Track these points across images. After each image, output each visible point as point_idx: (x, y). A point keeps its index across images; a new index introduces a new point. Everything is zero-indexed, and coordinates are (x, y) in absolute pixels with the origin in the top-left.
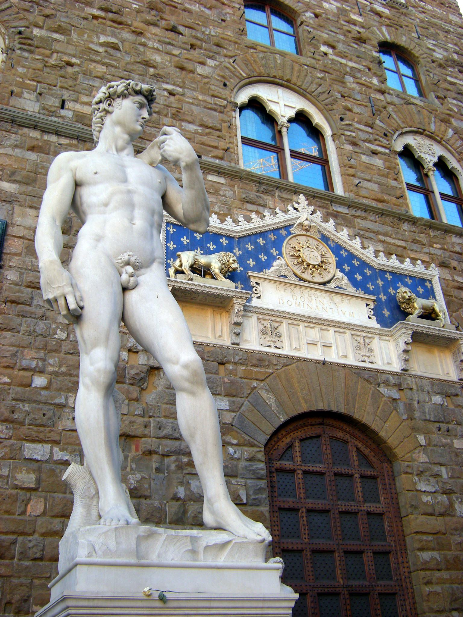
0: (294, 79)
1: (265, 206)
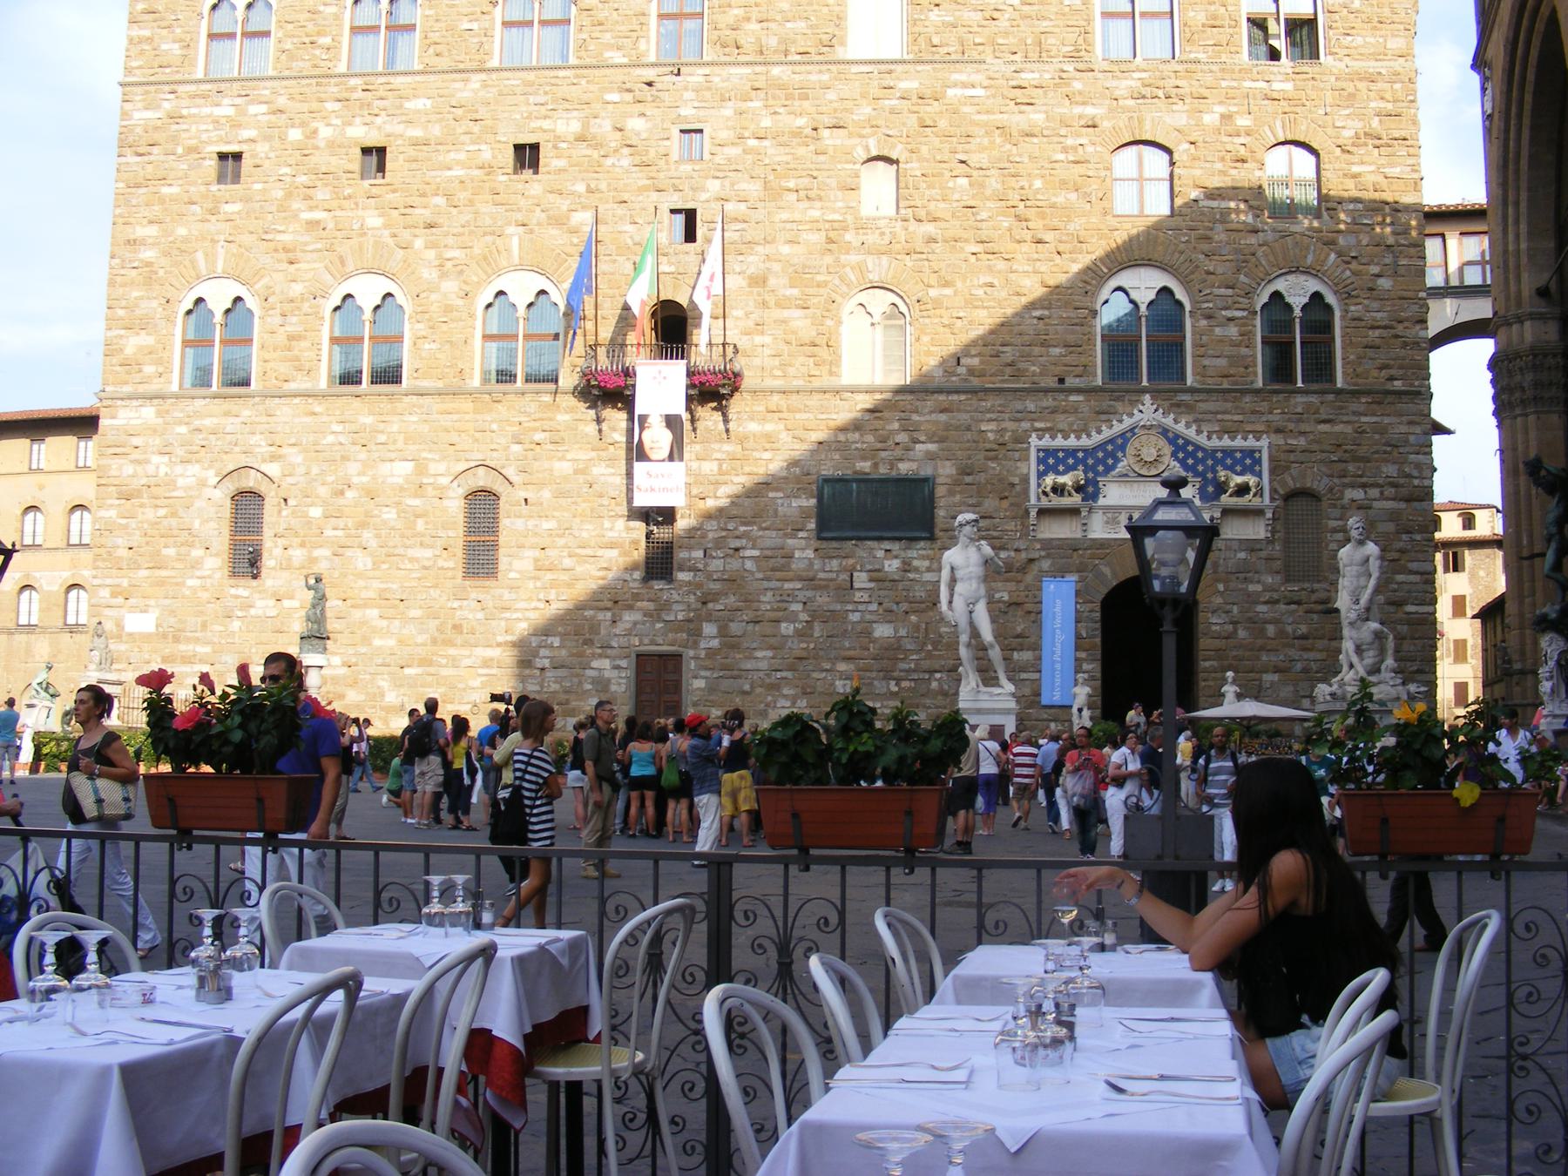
0: (1156, 256)
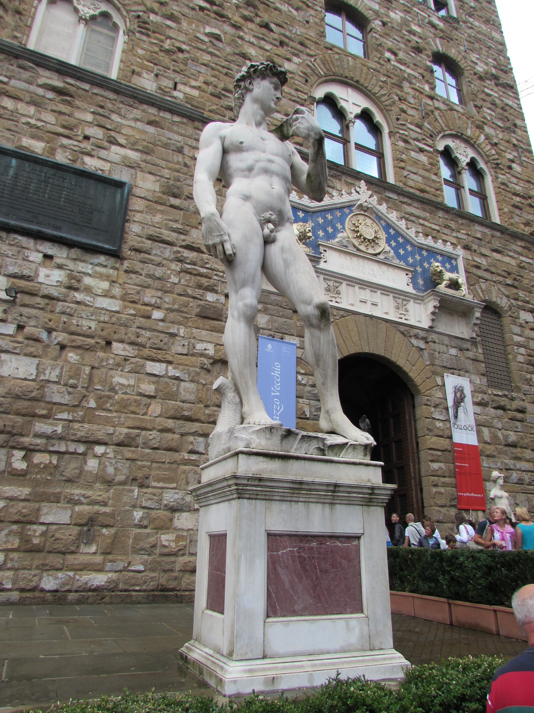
0: (362, 81)
1: (333, 188)
